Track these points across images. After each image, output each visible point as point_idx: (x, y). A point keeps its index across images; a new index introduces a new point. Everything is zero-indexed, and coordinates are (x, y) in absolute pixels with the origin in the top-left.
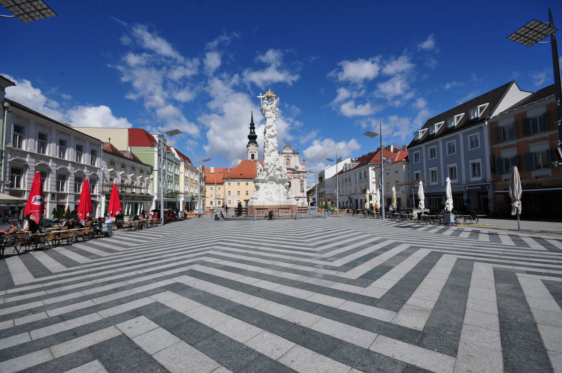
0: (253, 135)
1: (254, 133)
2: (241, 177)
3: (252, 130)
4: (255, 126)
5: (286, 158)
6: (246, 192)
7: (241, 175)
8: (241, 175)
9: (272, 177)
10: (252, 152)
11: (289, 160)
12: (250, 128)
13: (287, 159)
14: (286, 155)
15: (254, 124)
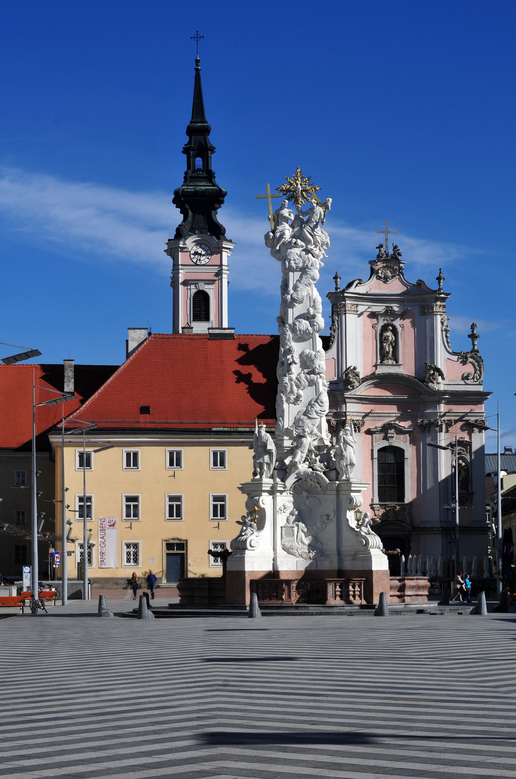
0: (203, 186)
1: (210, 176)
2: (144, 420)
3: (199, 162)
4: (212, 139)
5: (382, 322)
6: (172, 499)
7: (145, 410)
8: (145, 410)
9: (306, 474)
10: (195, 282)
11: (395, 331)
12: (186, 151)
13: (384, 328)
14: (380, 308)
15: (206, 131)
